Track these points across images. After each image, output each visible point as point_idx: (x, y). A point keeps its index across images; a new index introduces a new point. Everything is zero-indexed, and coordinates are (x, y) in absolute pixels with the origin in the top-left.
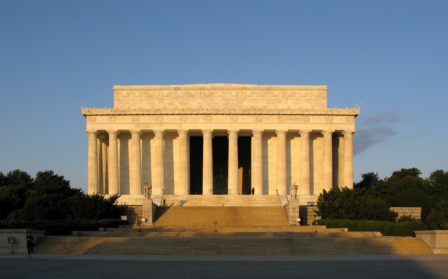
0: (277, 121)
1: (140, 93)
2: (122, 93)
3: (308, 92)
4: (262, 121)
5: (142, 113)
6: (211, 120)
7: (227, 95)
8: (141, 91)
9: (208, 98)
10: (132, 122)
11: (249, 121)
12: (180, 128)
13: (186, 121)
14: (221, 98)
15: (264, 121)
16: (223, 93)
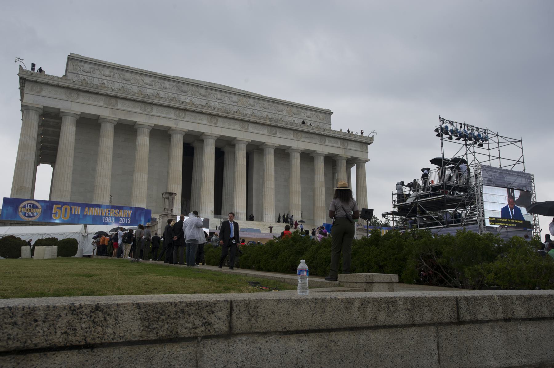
0: (292, 137)
1: (111, 72)
2: (83, 66)
3: (314, 113)
4: (275, 134)
5: (123, 95)
6: (216, 123)
7: (226, 98)
8: (112, 70)
9: (204, 98)
10: (105, 106)
11: (261, 132)
12: (175, 126)
13: (183, 118)
14: (219, 101)
15: (278, 134)
16: (222, 95)
